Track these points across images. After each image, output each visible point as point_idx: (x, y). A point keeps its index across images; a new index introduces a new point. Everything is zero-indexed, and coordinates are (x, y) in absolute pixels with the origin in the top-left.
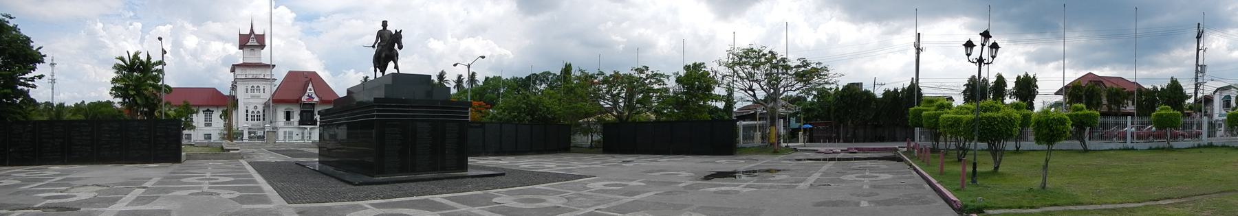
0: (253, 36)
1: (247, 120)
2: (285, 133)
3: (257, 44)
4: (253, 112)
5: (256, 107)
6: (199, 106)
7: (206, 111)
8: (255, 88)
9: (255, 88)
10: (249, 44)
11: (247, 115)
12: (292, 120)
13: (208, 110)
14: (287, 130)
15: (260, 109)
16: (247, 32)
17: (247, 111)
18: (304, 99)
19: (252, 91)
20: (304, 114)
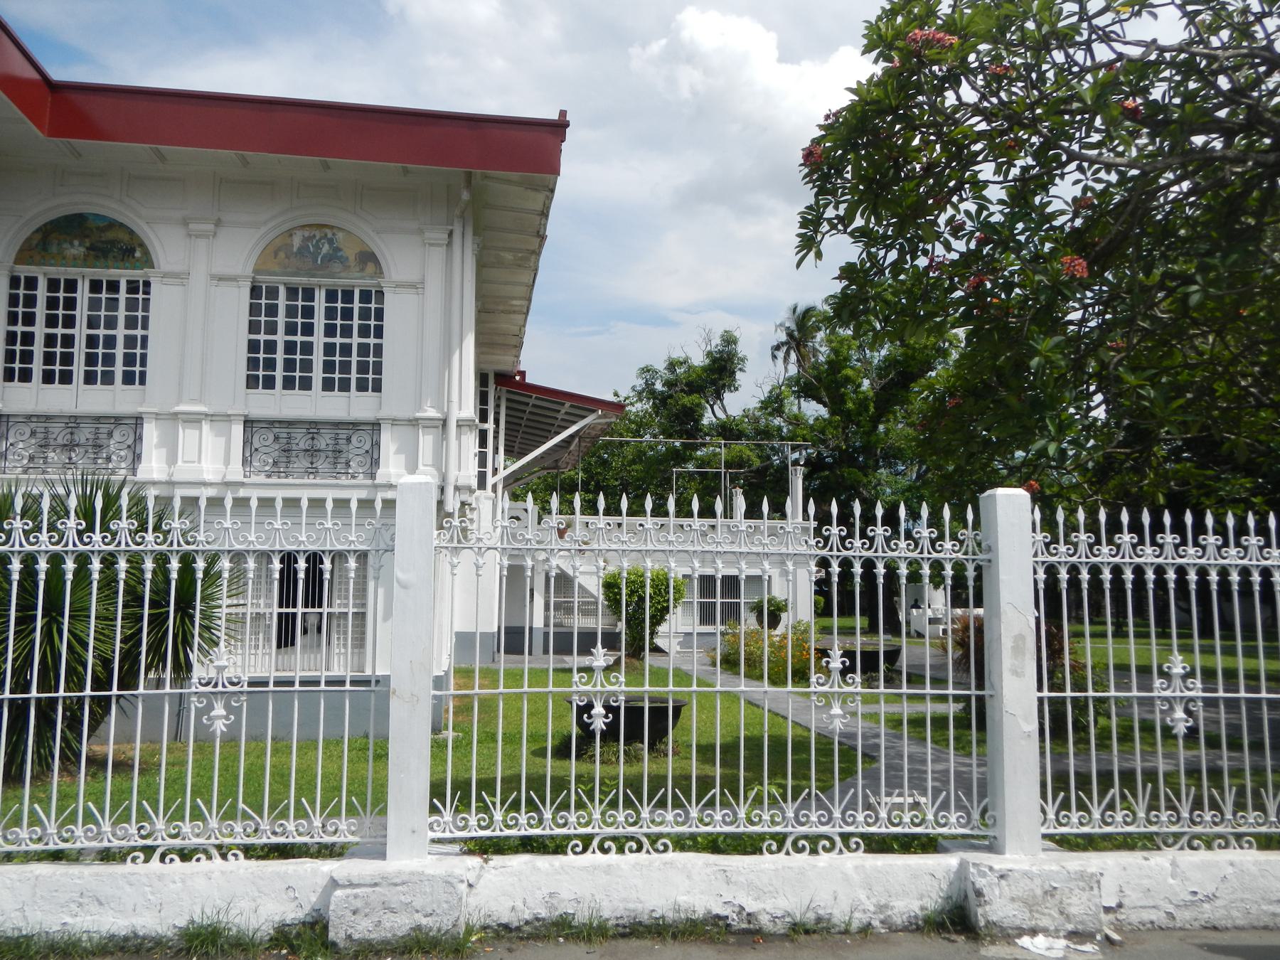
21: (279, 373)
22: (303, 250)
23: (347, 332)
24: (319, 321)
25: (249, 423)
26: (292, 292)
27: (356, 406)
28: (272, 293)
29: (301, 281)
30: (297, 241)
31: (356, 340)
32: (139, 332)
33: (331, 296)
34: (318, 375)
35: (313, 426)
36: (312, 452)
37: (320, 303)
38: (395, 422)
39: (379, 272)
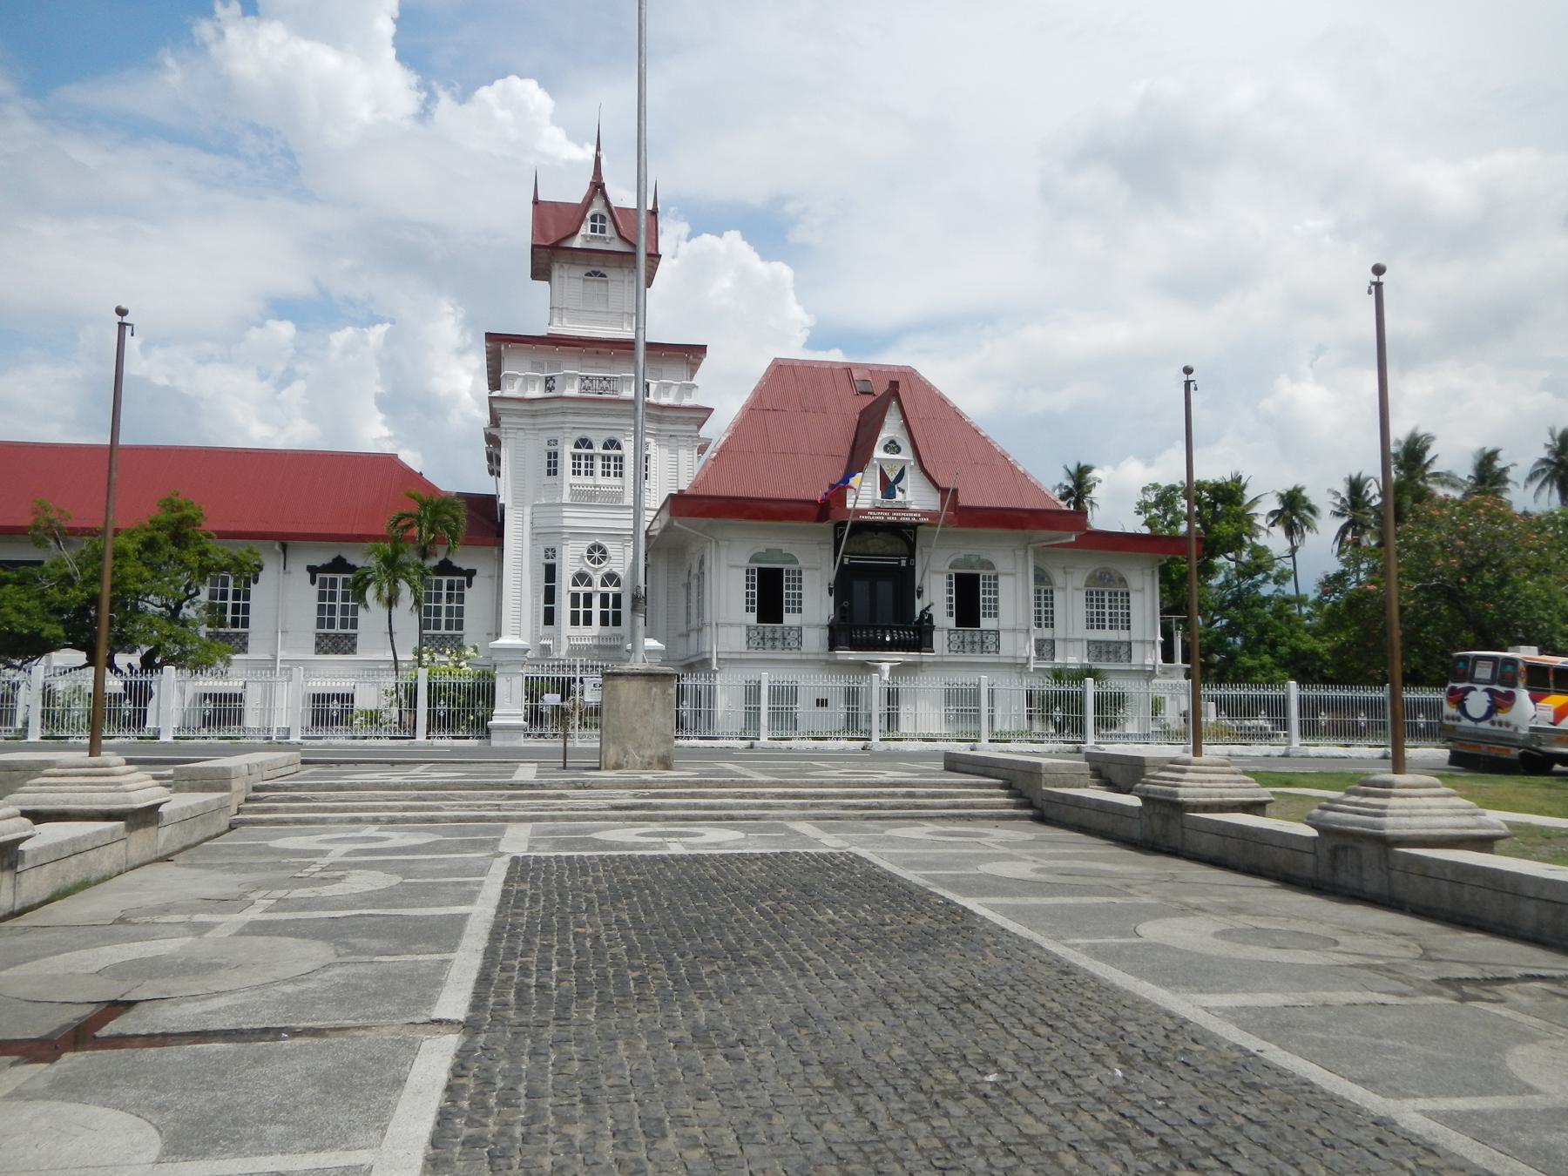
0: (597, 207)
1: (549, 618)
2: (752, 693)
3: (617, 246)
4: (581, 578)
5: (597, 553)
6: (286, 542)
7: (325, 569)
8: (598, 449)
9: (598, 449)
10: (577, 243)
11: (550, 595)
12: (789, 619)
13: (339, 565)
14: (766, 678)
15: (621, 559)
16: (577, 195)
17: (550, 572)
18: (864, 495)
19: (583, 464)
20: (860, 588)
21: (1095, 623)
22: (1100, 576)
23: (1116, 607)
24: (1107, 604)
25: (1088, 642)
26: (1097, 594)
27: (1123, 636)
28: (1091, 594)
29: (1103, 589)
30: (1098, 574)
31: (1120, 611)
32: (1049, 609)
33: (1110, 594)
34: (1107, 624)
35: (1108, 643)
36: (1108, 652)
37: (1107, 597)
38: (1137, 641)
39: (1126, 585)
